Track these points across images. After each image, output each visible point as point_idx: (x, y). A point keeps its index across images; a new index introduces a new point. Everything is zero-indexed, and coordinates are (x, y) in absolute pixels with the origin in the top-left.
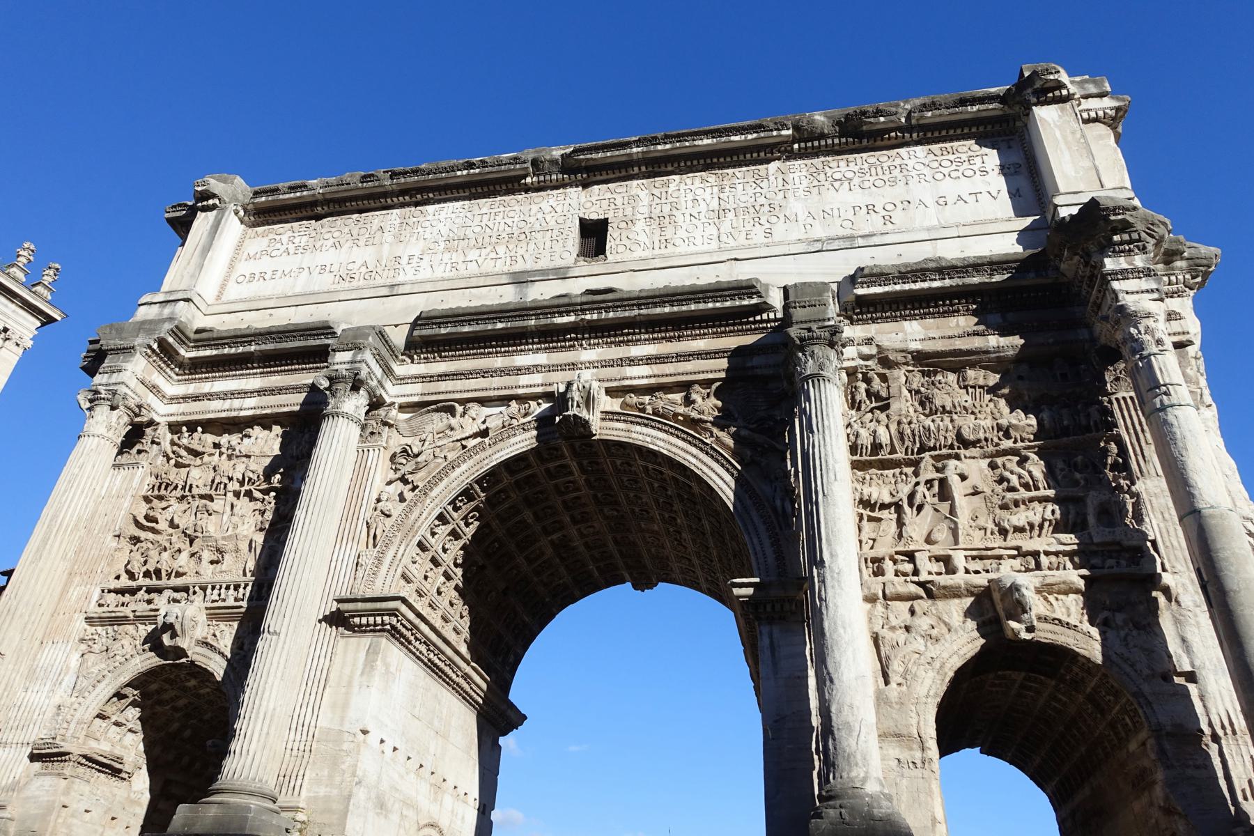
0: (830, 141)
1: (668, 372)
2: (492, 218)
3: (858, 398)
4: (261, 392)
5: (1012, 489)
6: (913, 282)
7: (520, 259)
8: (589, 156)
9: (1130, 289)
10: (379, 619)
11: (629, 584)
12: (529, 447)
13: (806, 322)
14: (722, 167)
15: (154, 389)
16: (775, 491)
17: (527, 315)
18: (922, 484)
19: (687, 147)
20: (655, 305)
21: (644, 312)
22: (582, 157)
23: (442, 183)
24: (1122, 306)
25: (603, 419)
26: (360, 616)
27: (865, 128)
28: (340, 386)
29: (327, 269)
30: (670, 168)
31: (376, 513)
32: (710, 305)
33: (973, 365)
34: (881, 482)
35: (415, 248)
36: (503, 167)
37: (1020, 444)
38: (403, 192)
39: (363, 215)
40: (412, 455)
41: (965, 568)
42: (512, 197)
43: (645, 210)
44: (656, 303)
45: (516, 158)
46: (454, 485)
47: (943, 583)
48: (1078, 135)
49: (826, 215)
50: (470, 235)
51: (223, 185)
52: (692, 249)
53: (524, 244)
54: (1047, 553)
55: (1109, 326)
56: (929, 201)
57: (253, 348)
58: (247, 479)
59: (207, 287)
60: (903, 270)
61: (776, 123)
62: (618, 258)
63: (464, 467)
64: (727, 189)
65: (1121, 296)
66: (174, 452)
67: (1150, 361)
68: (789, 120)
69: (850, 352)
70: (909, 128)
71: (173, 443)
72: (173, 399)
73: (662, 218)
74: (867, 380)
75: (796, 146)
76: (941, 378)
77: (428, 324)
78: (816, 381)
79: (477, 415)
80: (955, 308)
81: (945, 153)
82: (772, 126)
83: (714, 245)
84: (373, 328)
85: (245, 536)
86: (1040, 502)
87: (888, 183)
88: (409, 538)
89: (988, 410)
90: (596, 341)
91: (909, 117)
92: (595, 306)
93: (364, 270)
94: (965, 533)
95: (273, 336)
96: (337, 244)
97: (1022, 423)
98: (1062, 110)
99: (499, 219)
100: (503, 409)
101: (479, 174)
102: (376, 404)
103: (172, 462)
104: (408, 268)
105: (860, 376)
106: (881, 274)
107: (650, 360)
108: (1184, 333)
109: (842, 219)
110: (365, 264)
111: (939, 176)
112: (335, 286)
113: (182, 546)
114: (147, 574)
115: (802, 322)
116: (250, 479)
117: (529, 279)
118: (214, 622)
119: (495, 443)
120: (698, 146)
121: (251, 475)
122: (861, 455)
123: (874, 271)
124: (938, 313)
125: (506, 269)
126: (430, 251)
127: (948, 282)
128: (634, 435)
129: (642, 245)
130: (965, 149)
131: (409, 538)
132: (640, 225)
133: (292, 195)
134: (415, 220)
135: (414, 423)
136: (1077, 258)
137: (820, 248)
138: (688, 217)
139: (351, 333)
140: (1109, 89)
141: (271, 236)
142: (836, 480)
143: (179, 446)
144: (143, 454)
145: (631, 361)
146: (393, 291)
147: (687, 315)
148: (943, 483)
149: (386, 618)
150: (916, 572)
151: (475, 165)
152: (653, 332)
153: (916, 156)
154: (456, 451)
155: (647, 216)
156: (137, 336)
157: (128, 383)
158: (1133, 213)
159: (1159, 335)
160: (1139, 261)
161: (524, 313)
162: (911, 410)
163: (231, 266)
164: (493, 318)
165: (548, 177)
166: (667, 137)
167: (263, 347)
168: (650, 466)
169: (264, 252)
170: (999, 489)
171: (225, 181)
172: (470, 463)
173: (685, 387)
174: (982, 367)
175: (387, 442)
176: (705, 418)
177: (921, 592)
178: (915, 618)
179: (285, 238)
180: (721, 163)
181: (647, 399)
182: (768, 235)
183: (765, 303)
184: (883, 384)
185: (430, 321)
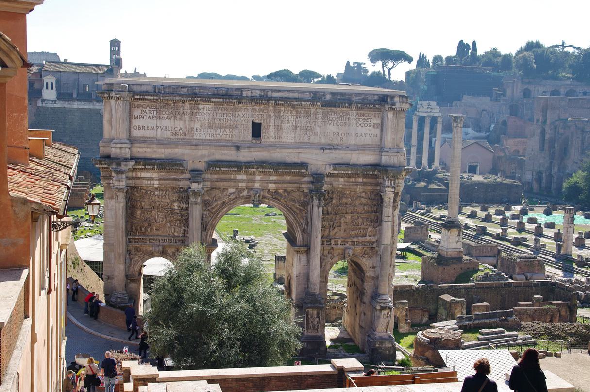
4: (160, 179)
5: (354, 225)
29: (167, 128)
35: (197, 125)
43: (273, 122)
63: (225, 209)
93: (181, 130)
98: (394, 114)
99: (225, 116)
125: (230, 139)
130: (367, 115)
132: (271, 127)
141: (141, 108)
145: (270, 183)
150: (331, 244)
172: (227, 208)
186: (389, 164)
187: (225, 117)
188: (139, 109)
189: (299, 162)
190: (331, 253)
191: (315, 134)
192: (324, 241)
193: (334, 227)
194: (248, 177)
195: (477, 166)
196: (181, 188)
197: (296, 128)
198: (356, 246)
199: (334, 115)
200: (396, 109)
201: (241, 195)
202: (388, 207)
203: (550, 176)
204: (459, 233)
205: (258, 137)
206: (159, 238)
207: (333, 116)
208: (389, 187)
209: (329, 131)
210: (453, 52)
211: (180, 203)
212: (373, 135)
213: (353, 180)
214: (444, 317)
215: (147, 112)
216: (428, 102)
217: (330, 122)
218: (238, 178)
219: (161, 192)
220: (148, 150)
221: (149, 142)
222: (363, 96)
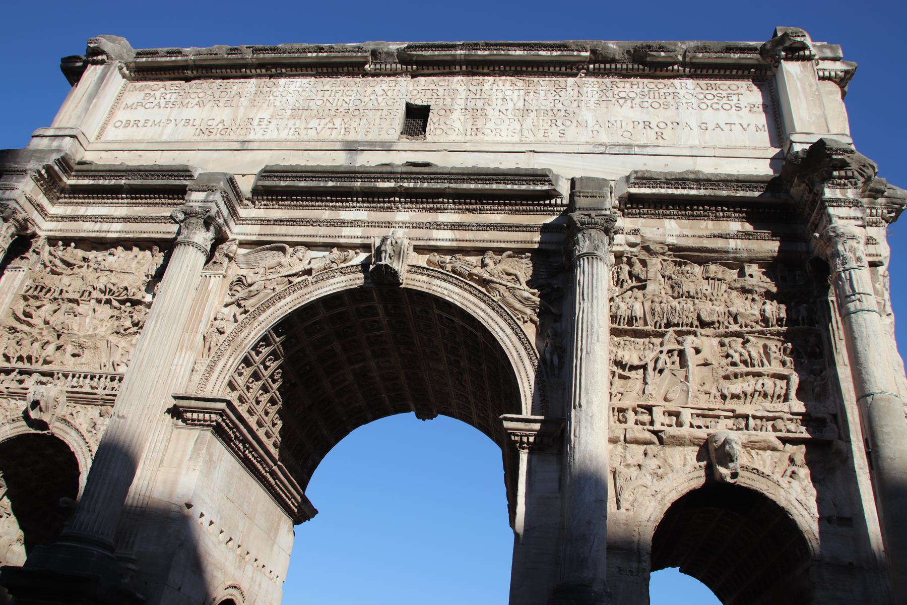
0: (619, 66)
1: (468, 238)
2: (333, 94)
3: (621, 277)
4: (126, 219)
5: (734, 364)
6: (675, 188)
7: (352, 131)
8: (420, 53)
9: (841, 215)
10: (207, 416)
11: (413, 414)
12: (345, 288)
13: (587, 209)
14: (529, 74)
15: (39, 208)
16: (547, 346)
17: (354, 178)
18: (665, 352)
19: (502, 55)
20: (463, 181)
21: (453, 186)
22: (414, 53)
23: (294, 61)
24: (834, 228)
25: (410, 272)
26: (193, 412)
27: (648, 59)
28: (193, 220)
29: (191, 122)
30: (486, 71)
31: (211, 329)
32: (509, 187)
33: (715, 261)
34: (632, 348)
36: (347, 54)
37: (744, 329)
38: (261, 65)
39: (226, 81)
40: (246, 285)
41: (691, 423)
42: (352, 79)
43: (462, 102)
44: (464, 179)
45: (359, 48)
46: (279, 312)
47: (672, 433)
48: (814, 88)
49: (611, 125)
50: (313, 107)
51: (112, 44)
52: (498, 139)
53: (357, 120)
54: (754, 417)
55: (822, 242)
56: (694, 126)
57: (123, 182)
58: (108, 290)
59: (91, 130)
60: (670, 178)
61: (577, 46)
62: (436, 139)
63: (288, 299)
64: (532, 93)
65: (834, 219)
66: (51, 262)
67: (850, 274)
68: (589, 44)
69: (619, 238)
70: (683, 64)
71: (51, 254)
72: (53, 217)
73: (475, 111)
74: (630, 263)
75: (591, 66)
76: (689, 269)
77: (271, 177)
78: (590, 259)
79: (303, 257)
80: (706, 213)
81: (710, 88)
82: (574, 47)
83: (516, 138)
84: (225, 174)
85: (103, 337)
86: (754, 376)
87: (662, 106)
88: (238, 353)
89: (723, 300)
90: (410, 205)
91: (684, 56)
92: (413, 176)
94: (694, 395)
95: (141, 173)
96: (201, 103)
97: (748, 312)
98: (804, 67)
99: (338, 96)
100: (327, 253)
101: (327, 57)
102: (220, 239)
103: (48, 269)
104: (257, 128)
105: (625, 259)
106: (651, 179)
107: (454, 227)
108: (877, 255)
109: (623, 130)
110: (222, 122)
111: (704, 106)
112: (195, 138)
113: (51, 339)
114: (20, 359)
115: (583, 209)
116: (111, 290)
117: (359, 148)
118: (72, 404)
119: (317, 282)
120: (512, 55)
121: (112, 287)
122: (619, 324)
123: (646, 175)
124: (693, 216)
125: (340, 138)
126: (278, 117)
127: (702, 192)
128: (434, 288)
129: (457, 130)
130: (726, 87)
131: (238, 353)
132: (456, 115)
133: (168, 59)
134: (268, 89)
135: (250, 258)
136: (804, 185)
137: (604, 150)
139: (206, 177)
140: (841, 55)
141: (147, 91)
142: (598, 341)
143: (55, 257)
144: (25, 260)
145: (438, 226)
146: (244, 146)
147: (489, 192)
148: (681, 353)
149: (213, 416)
150: (652, 423)
151: (323, 49)
152: (460, 203)
153: (686, 87)
154: (283, 285)
155: (463, 107)
156: (29, 162)
157: (19, 200)
158: (850, 155)
159: (858, 254)
160: (851, 194)
161: (353, 175)
162: (663, 292)
163: (112, 113)
164: (325, 177)
165: (383, 66)
166: (487, 45)
167: (132, 182)
168: (445, 315)
170: (724, 362)
171: (113, 42)
173: (481, 251)
174: (722, 264)
175: (226, 272)
176: (495, 280)
177: (654, 439)
178: (647, 459)
179: (158, 94)
180: (529, 72)
181: (448, 258)
182: (562, 135)
183: (554, 190)
184: (643, 269)
185: (273, 174)
212: (752, 127)
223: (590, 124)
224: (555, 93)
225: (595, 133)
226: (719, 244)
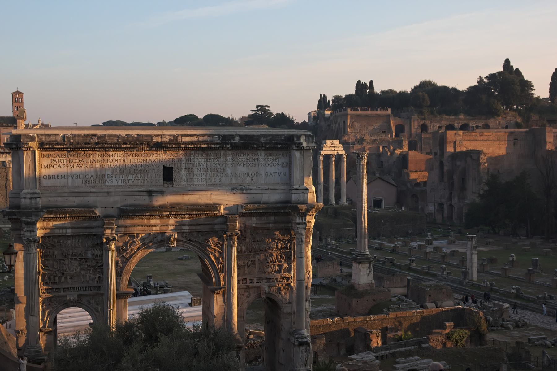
2: (134, 162)
4: (72, 228)
7: (146, 180)
29: (78, 176)
43: (184, 165)
52: (198, 183)
63: (140, 254)
93: (92, 178)
98: (301, 153)
104: (108, 180)
125: (142, 184)
130: (275, 155)
132: (183, 171)
138: (197, 170)
141: (51, 158)
150: (246, 283)
153: (262, 155)
169: (50, 166)
181: (187, 234)
186: (299, 201)
187: (136, 163)
188: (48, 159)
189: (212, 202)
190: (247, 292)
191: (226, 175)
192: (240, 280)
193: (249, 266)
194: (162, 220)
195: (381, 200)
196: (95, 235)
197: (206, 170)
198: (271, 283)
199: (243, 156)
200: (303, 148)
201: (155, 239)
202: (301, 243)
203: (451, 206)
204: (370, 266)
205: (170, 181)
206: (73, 287)
207: (242, 158)
208: (300, 223)
209: (239, 172)
210: (353, 91)
211: (94, 250)
212: (282, 174)
213: (265, 218)
214: (361, 349)
215: (57, 161)
216: (331, 141)
217: (240, 163)
218: (151, 223)
219: (74, 240)
220: (59, 199)
221: (59, 191)
222: (271, 137)
223: (229, 175)
224: (217, 160)
225: (231, 179)
226: (267, 225)
